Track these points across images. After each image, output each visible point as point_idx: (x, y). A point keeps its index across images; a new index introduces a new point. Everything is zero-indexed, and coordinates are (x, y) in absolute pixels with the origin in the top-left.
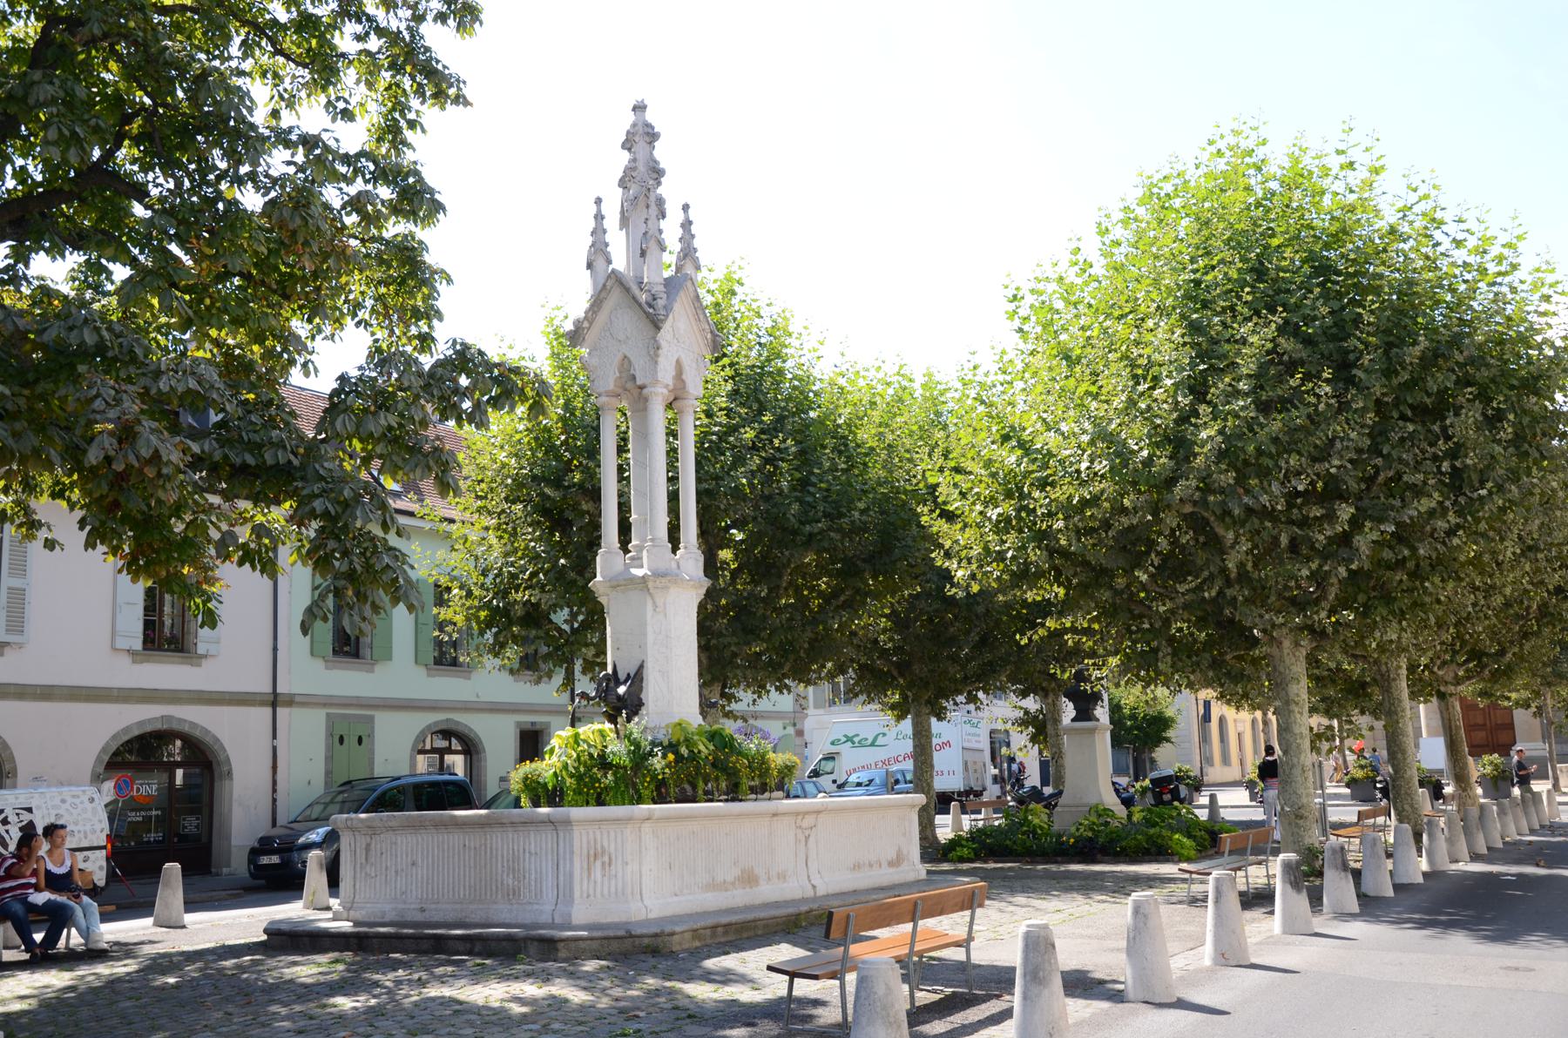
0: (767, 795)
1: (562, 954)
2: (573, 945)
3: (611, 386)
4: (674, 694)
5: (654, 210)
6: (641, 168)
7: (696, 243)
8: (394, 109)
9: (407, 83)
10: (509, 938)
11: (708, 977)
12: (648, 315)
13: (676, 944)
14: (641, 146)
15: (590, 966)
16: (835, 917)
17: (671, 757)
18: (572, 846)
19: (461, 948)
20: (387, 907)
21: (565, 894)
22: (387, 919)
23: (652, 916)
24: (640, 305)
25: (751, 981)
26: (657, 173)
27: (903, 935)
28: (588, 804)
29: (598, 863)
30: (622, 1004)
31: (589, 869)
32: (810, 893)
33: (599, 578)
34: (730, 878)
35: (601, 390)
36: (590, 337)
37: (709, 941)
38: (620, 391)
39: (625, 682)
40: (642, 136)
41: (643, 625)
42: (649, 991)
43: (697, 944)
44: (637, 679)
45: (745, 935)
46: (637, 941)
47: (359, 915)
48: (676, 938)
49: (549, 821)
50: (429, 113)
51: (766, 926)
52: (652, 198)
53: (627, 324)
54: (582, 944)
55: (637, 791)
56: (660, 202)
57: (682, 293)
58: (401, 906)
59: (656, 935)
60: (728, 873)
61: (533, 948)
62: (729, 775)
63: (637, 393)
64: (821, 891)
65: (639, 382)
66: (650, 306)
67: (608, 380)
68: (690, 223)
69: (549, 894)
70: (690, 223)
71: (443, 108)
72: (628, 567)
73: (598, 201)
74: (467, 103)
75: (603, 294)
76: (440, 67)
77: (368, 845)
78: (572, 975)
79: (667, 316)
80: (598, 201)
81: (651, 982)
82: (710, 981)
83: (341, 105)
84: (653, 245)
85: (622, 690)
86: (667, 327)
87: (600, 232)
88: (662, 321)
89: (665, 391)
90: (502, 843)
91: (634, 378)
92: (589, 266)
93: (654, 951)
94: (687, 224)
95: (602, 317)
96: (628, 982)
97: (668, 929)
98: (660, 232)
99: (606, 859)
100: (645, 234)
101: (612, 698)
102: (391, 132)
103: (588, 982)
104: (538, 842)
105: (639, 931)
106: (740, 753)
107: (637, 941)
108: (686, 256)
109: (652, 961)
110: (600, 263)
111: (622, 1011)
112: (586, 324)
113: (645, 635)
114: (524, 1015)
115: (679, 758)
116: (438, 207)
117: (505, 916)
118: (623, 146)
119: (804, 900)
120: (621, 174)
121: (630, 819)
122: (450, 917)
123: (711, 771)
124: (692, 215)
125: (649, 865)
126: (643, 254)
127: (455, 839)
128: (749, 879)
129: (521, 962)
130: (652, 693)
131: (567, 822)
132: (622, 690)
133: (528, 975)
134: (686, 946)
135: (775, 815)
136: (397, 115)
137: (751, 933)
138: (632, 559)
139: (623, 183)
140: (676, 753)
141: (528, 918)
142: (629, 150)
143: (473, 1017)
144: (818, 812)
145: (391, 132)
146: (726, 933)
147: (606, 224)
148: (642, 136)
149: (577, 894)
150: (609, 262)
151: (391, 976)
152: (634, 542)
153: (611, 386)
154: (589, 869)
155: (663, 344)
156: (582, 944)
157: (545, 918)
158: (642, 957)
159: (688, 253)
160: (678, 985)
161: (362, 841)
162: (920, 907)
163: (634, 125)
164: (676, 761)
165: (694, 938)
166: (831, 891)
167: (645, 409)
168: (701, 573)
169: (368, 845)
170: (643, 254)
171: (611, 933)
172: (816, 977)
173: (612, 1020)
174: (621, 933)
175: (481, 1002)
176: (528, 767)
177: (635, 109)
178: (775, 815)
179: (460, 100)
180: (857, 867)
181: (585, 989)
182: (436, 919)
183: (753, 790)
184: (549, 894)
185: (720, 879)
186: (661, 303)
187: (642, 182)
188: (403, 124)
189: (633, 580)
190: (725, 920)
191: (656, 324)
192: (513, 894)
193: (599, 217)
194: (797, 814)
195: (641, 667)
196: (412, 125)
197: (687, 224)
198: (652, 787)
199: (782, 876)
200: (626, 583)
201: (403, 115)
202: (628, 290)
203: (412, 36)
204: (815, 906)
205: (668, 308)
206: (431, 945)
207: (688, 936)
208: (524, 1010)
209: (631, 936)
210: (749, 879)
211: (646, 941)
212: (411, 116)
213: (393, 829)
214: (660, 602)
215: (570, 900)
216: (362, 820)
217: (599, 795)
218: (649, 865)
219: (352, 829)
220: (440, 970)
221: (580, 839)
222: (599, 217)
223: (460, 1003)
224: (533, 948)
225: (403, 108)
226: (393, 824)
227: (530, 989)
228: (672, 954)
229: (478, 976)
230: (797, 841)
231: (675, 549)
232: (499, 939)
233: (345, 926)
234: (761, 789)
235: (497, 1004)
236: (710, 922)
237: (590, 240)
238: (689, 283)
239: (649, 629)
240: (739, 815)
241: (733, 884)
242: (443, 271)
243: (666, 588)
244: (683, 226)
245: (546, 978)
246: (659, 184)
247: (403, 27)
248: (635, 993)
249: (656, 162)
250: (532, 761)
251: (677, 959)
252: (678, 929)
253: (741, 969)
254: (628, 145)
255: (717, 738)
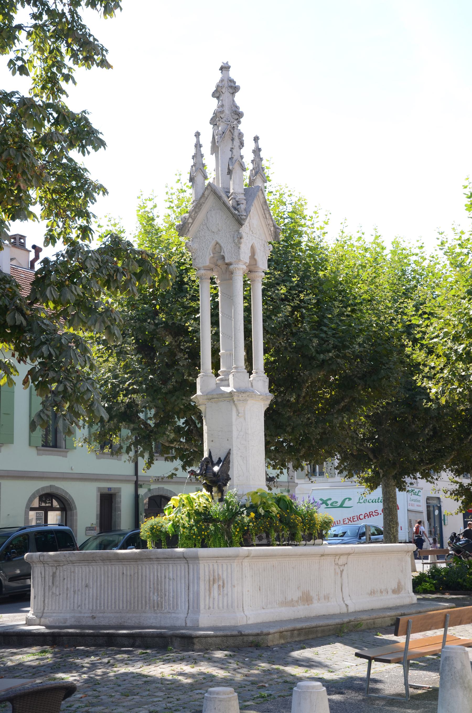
0: (312, 542)
1: (197, 647)
2: (204, 640)
3: (207, 263)
4: (251, 473)
5: (237, 143)
6: (227, 112)
7: (264, 163)
8: (53, 65)
9: (63, 49)
10: (161, 636)
11: (297, 662)
12: (233, 215)
13: (273, 641)
14: (226, 95)
15: (219, 654)
16: (401, 622)
17: (253, 515)
18: (198, 573)
19: (126, 643)
20: (68, 616)
21: (193, 606)
22: (68, 624)
23: (250, 622)
24: (228, 208)
25: (326, 666)
26: (238, 115)
27: (438, 637)
28: (195, 546)
29: (216, 586)
30: (251, 679)
31: (210, 590)
32: (344, 610)
33: (199, 392)
34: (295, 599)
35: (200, 265)
36: (193, 229)
37: (289, 640)
38: (212, 266)
39: (218, 464)
40: (227, 88)
41: (231, 425)
42: (264, 671)
43: (282, 641)
44: (226, 461)
45: (311, 637)
46: (245, 639)
47: (47, 621)
48: (270, 636)
49: (184, 557)
50: (79, 72)
51: (323, 631)
52: (236, 134)
53: (218, 221)
54: (210, 640)
55: (230, 538)
56: (241, 135)
57: (255, 201)
58: (78, 615)
59: (258, 635)
60: (295, 595)
61: (177, 642)
62: (290, 527)
63: (227, 270)
64: (351, 609)
65: (227, 261)
66: (236, 209)
67: (205, 259)
68: (260, 150)
69: (183, 607)
70: (260, 150)
71: (89, 68)
72: (218, 386)
73: (198, 135)
74: (109, 66)
75: (202, 200)
76: (91, 39)
77: (54, 574)
78: (210, 660)
79: (247, 216)
80: (198, 135)
81: (264, 665)
82: (300, 666)
83: (19, 63)
84: (237, 167)
85: (216, 469)
86: (246, 223)
87: (199, 156)
88: (244, 220)
89: (244, 267)
90: (149, 571)
91: (223, 258)
92: (192, 179)
93: (257, 646)
94: (257, 151)
95: (201, 215)
96: (250, 666)
97: (265, 631)
98: (242, 157)
99: (221, 583)
100: (231, 159)
101: (210, 475)
102: (51, 83)
103: (221, 664)
104: (175, 571)
105: (246, 632)
106: (296, 513)
107: (245, 639)
108: (256, 173)
109: (258, 652)
110: (199, 178)
111: (253, 683)
112: (190, 220)
113: (231, 432)
114: (191, 684)
115: (258, 516)
116: (99, 144)
117: (153, 621)
118: (214, 95)
119: (341, 615)
120: (211, 115)
121: (236, 557)
122: (113, 622)
123: (282, 525)
124: (261, 144)
125: (245, 588)
126: (230, 172)
127: (117, 569)
128: (307, 599)
129: (171, 651)
130: (236, 471)
131: (196, 558)
132: (216, 469)
133: (182, 660)
134: (276, 643)
135: (322, 555)
136: (54, 70)
137: (314, 636)
138: (221, 380)
139: (213, 121)
140: (256, 512)
141: (168, 622)
142: (218, 98)
143: (160, 685)
144: (349, 554)
145: (51, 83)
146: (299, 635)
147: (203, 150)
148: (227, 88)
149: (202, 606)
150: (206, 178)
151: (87, 660)
152: (222, 369)
153: (207, 263)
154: (210, 590)
155: (244, 235)
156: (210, 640)
157: (180, 623)
158: (250, 649)
159: (258, 170)
160: (281, 668)
161: (50, 571)
162: (448, 619)
163: (222, 81)
164: (256, 518)
165: (281, 637)
166: (357, 609)
167: (231, 279)
168: (267, 390)
169: (54, 574)
170: (230, 172)
171: (229, 633)
172: (389, 662)
173: (250, 688)
174: (235, 633)
175: (159, 676)
176: (153, 521)
177: (222, 69)
178: (322, 555)
179: (104, 64)
180: (372, 593)
181: (222, 668)
182: (103, 623)
183: (304, 538)
184: (183, 607)
185: (289, 599)
186: (243, 207)
187: (227, 121)
188: (59, 76)
189: (223, 394)
190: (299, 626)
191: (240, 222)
192: (157, 606)
193: (198, 146)
194: (336, 555)
195: (229, 453)
196: (67, 78)
197: (257, 151)
198: (240, 535)
199: (327, 598)
200: (217, 397)
201: (60, 72)
202: (220, 198)
203: (72, 17)
204: (352, 618)
205: (248, 211)
206: (107, 641)
207: (277, 636)
208: (189, 681)
209: (242, 635)
210: (307, 599)
211: (251, 638)
212: (65, 71)
213: (72, 562)
214: (241, 409)
215: (197, 610)
216: (51, 556)
217: (203, 540)
218: (245, 588)
219: (43, 563)
220: (119, 656)
221: (204, 569)
222: (198, 146)
223: (146, 676)
224: (177, 642)
225: (60, 65)
226: (74, 559)
227: (187, 668)
228: (268, 648)
229: (148, 660)
230: (336, 573)
231: (250, 373)
232: (152, 636)
233: (42, 629)
234: (309, 537)
235: (170, 677)
236: (290, 627)
237: (192, 162)
238: (260, 193)
239: (234, 428)
240: (301, 555)
241: (297, 602)
242: (101, 186)
243: (245, 400)
244: (254, 152)
245: (195, 662)
246: (239, 122)
247: (66, 10)
248: (256, 672)
249: (237, 107)
250: (156, 516)
251: (273, 651)
252: (272, 631)
253: (316, 658)
254: (217, 94)
255: (281, 503)
